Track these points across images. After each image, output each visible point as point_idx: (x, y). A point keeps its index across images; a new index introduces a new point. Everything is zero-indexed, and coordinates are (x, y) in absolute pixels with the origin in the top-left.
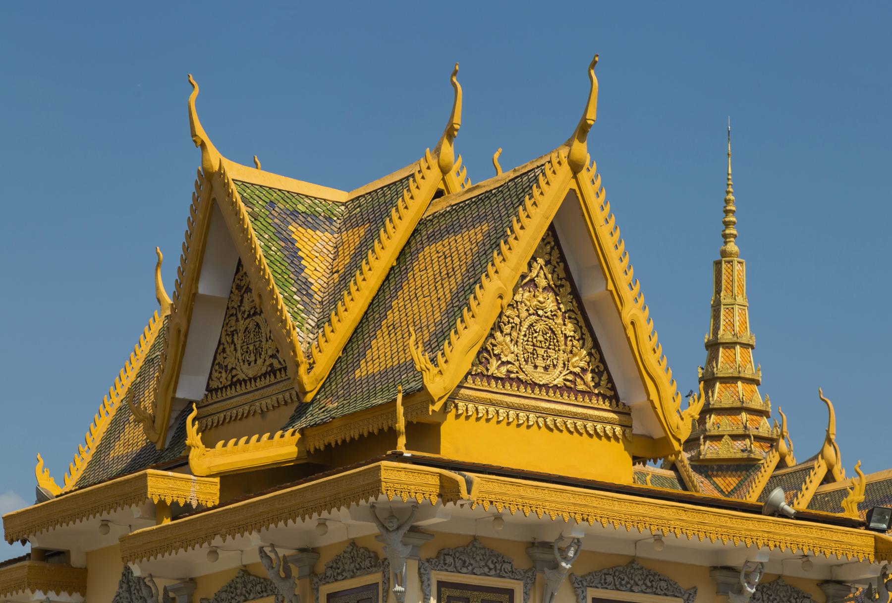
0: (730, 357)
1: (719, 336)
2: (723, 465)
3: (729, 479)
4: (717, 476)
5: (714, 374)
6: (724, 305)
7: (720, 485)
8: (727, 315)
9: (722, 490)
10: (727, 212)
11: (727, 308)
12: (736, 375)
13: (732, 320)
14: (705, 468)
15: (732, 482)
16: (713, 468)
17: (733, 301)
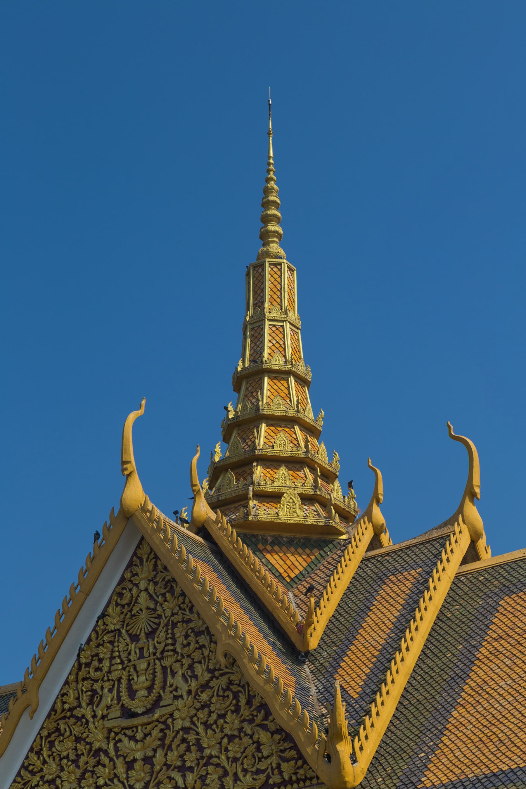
0: (280, 391)
1: (264, 359)
2: (282, 537)
3: (292, 558)
4: (269, 552)
5: (258, 409)
6: (270, 320)
7: (277, 566)
8: (273, 335)
9: (281, 574)
10: (267, 204)
11: (274, 326)
12: (292, 413)
13: (281, 343)
14: (254, 540)
15: (297, 564)
16: (266, 540)
17: (283, 316)
